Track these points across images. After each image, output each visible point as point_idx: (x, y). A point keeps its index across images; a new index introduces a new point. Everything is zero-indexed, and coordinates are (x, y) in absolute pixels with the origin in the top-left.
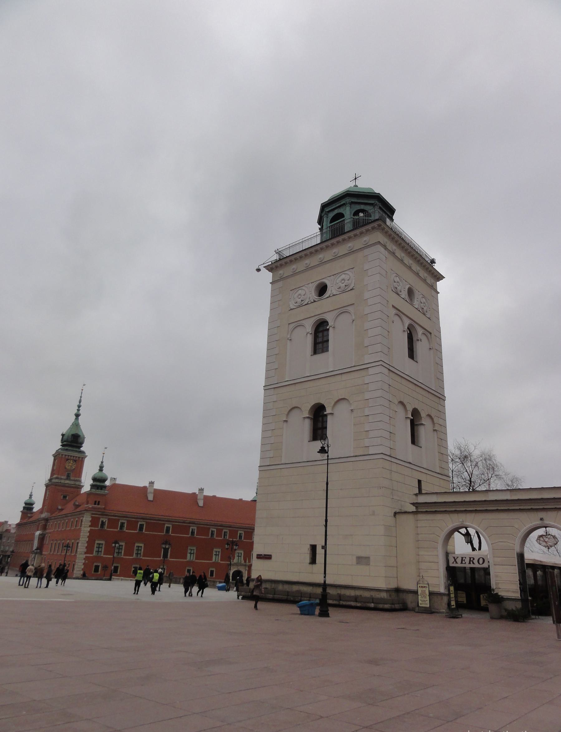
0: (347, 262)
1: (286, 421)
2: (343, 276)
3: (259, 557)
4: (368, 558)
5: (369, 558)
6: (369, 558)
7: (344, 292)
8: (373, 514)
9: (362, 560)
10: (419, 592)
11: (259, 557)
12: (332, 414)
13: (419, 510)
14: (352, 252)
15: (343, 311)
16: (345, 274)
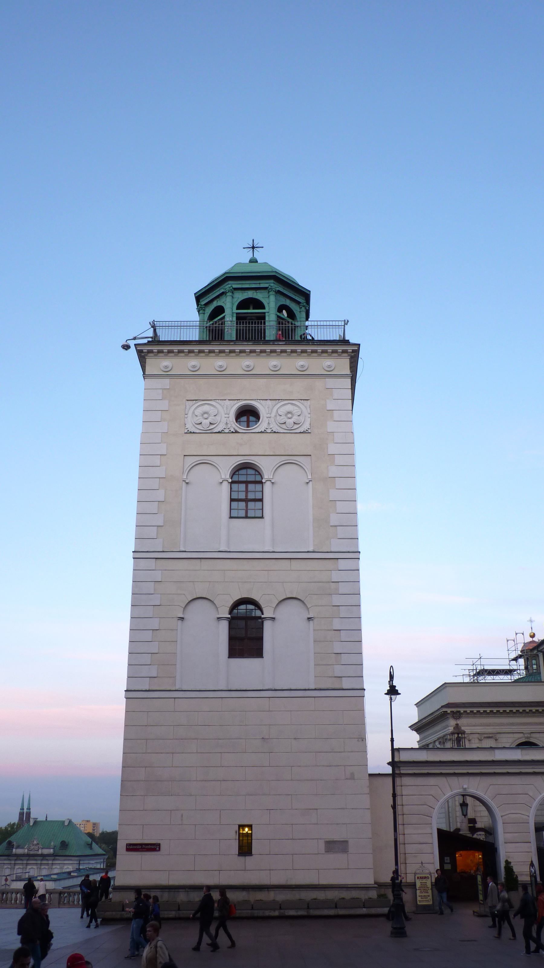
0: (298, 387)
1: (182, 619)
2: (289, 408)
3: (132, 848)
4: (345, 843)
5: (347, 842)
6: (347, 842)
7: (290, 431)
8: (352, 777)
9: (335, 846)
10: (418, 885)
11: (132, 848)
12: (273, 619)
13: (402, 772)
14: (302, 375)
15: (289, 460)
16: (292, 404)
